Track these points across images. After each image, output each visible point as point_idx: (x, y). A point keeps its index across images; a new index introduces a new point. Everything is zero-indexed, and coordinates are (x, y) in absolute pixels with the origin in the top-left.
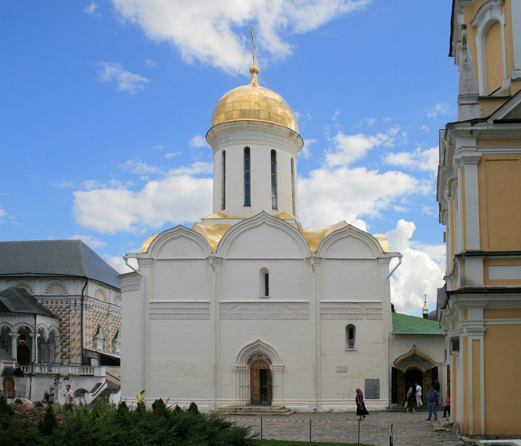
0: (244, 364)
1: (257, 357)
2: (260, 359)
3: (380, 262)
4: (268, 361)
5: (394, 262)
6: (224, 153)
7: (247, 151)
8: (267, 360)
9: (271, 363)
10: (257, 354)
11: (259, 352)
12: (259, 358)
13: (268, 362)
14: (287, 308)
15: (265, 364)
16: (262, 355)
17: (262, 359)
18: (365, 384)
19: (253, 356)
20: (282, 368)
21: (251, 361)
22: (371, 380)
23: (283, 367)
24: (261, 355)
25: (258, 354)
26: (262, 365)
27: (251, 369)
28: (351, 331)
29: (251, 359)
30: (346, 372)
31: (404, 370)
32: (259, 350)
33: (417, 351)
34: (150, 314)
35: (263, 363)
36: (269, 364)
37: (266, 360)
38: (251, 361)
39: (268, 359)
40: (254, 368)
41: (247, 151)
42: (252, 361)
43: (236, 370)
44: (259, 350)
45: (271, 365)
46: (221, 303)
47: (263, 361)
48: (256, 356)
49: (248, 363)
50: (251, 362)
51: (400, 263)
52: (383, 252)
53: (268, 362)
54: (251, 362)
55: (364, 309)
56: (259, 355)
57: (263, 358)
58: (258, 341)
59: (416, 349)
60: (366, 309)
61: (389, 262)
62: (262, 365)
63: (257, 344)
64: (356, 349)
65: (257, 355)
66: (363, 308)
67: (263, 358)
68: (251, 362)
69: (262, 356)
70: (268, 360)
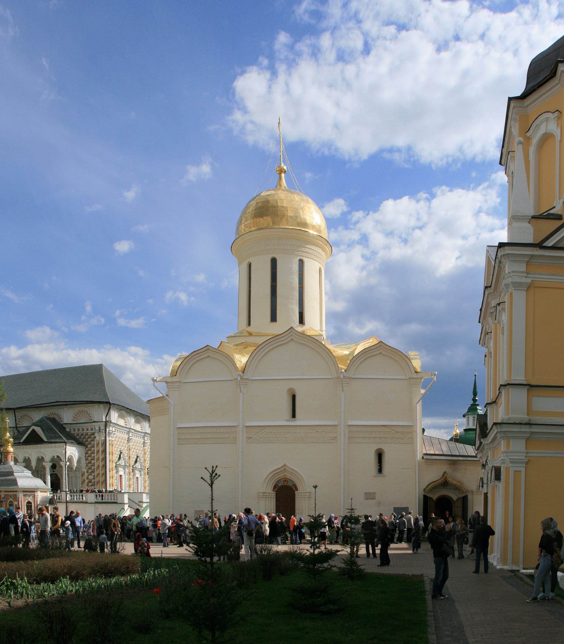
0: (270, 490)
1: (282, 482)
2: (286, 484)
8: (293, 485)
9: (297, 490)
12: (284, 483)
13: (294, 488)
14: (314, 431)
16: (288, 481)
19: (279, 481)
20: (309, 494)
23: (310, 493)
25: (284, 479)
28: (380, 456)
29: (277, 485)
30: (375, 499)
31: (434, 498)
32: (285, 475)
33: (448, 478)
36: (295, 490)
39: (294, 485)
43: (262, 496)
44: (285, 475)
46: (247, 426)
48: (282, 481)
53: (294, 488)
56: (285, 481)
57: (289, 483)
58: (285, 465)
59: (447, 476)
60: (396, 431)
63: (283, 469)
65: (283, 481)
66: (393, 432)
67: (290, 484)
68: (277, 489)
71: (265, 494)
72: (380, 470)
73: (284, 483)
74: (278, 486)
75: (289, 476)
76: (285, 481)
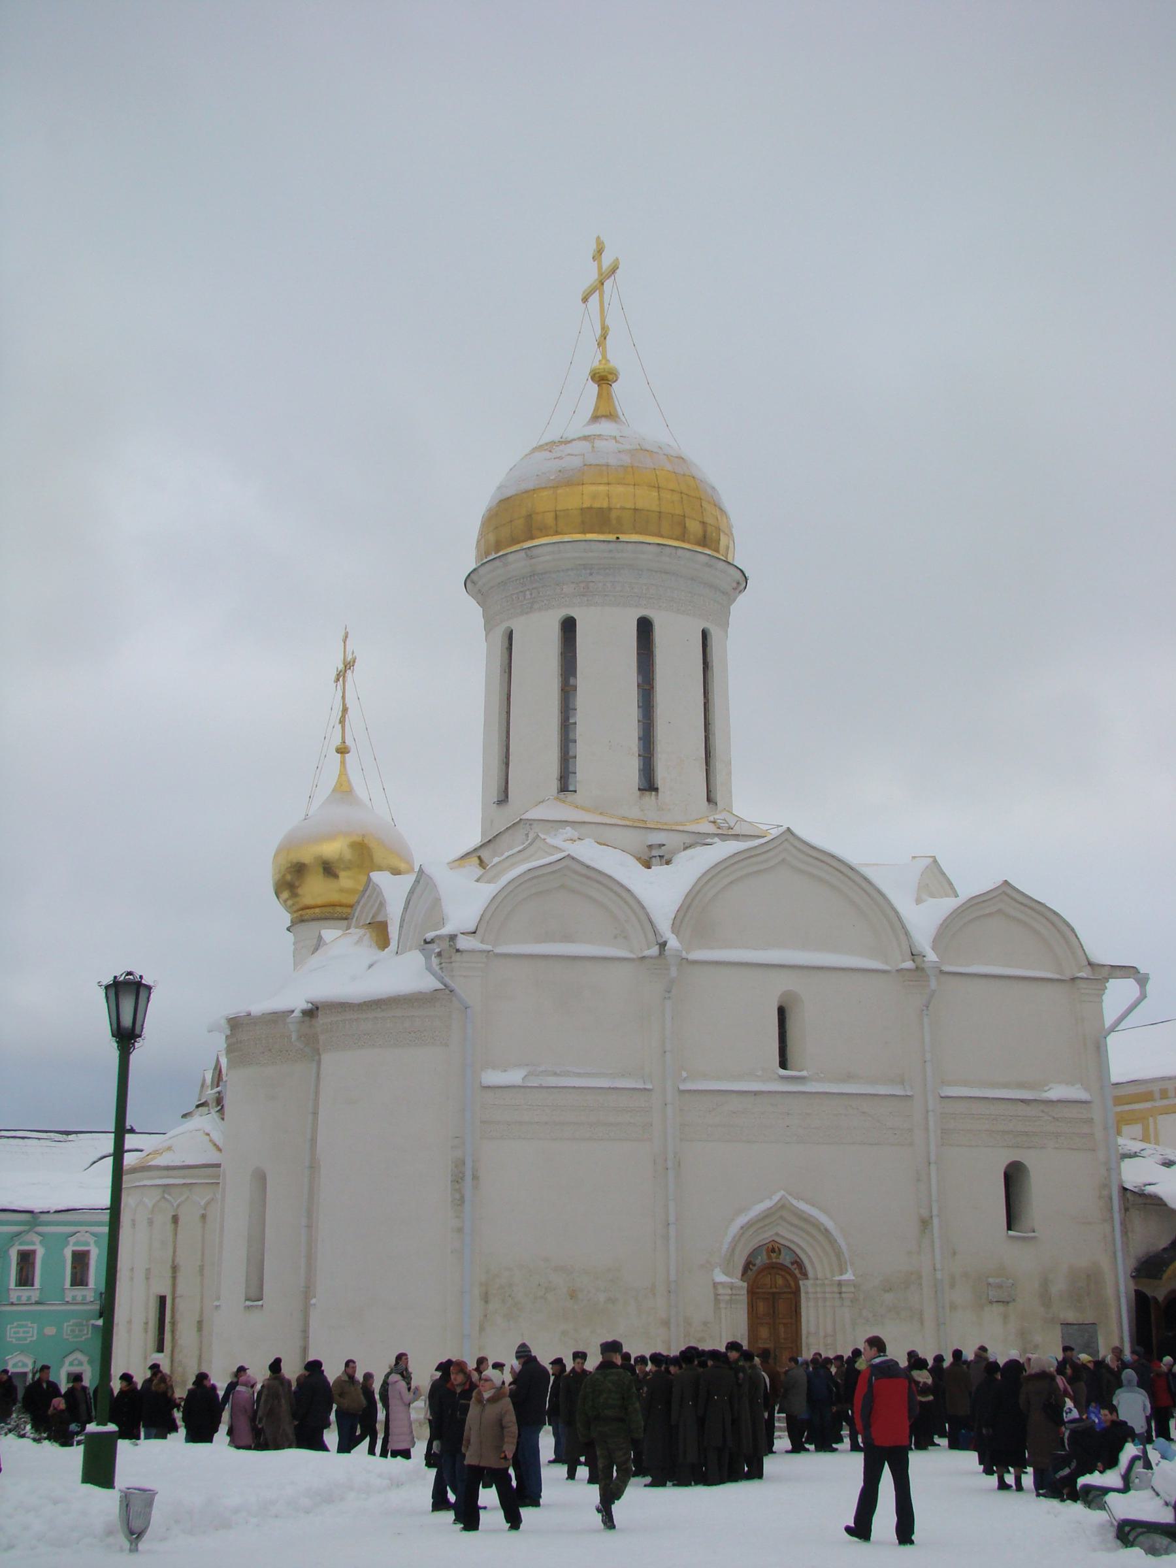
1: (765, 1257)
2: (774, 1260)
3: (1083, 991)
4: (795, 1269)
5: (1118, 993)
6: (569, 627)
7: (645, 628)
8: (793, 1264)
9: (805, 1275)
10: (766, 1246)
11: (770, 1242)
13: (797, 1272)
15: (788, 1277)
16: (780, 1250)
17: (780, 1261)
18: (1063, 1337)
20: (852, 1289)
21: (751, 1266)
22: (1075, 1327)
24: (777, 1249)
26: (780, 1281)
27: (752, 1293)
28: (1014, 1177)
31: (1160, 1299)
32: (777, 1234)
34: (481, 1122)
35: (783, 1273)
36: (799, 1276)
37: (790, 1266)
38: (751, 1266)
40: (758, 1290)
41: (645, 628)
42: (754, 1268)
45: (806, 1281)
47: (781, 1268)
48: (765, 1253)
49: (743, 1275)
50: (751, 1270)
51: (1143, 996)
52: (1090, 964)
54: (751, 1270)
55: (1050, 1118)
56: (773, 1251)
57: (782, 1257)
60: (1054, 1118)
61: (1102, 990)
62: (780, 1281)
64: (1032, 1234)
68: (749, 1273)
69: (780, 1254)
70: (795, 1266)
71: (734, 1292)
72: (1011, 1221)
73: (769, 1257)
74: (754, 1265)
75: (787, 1235)
76: (773, 1251)
